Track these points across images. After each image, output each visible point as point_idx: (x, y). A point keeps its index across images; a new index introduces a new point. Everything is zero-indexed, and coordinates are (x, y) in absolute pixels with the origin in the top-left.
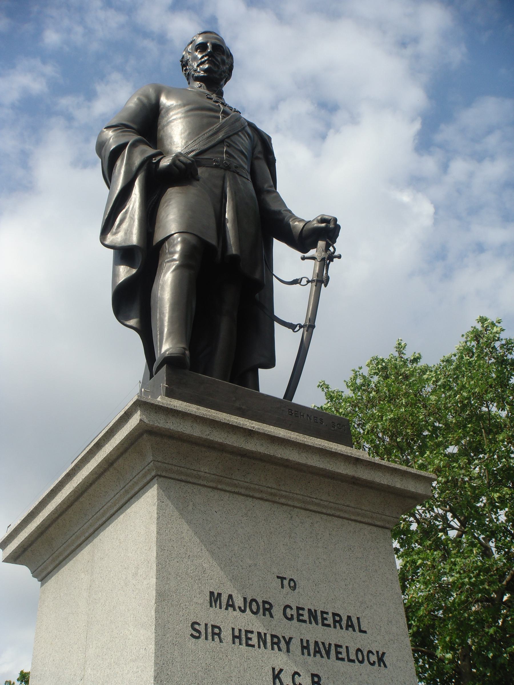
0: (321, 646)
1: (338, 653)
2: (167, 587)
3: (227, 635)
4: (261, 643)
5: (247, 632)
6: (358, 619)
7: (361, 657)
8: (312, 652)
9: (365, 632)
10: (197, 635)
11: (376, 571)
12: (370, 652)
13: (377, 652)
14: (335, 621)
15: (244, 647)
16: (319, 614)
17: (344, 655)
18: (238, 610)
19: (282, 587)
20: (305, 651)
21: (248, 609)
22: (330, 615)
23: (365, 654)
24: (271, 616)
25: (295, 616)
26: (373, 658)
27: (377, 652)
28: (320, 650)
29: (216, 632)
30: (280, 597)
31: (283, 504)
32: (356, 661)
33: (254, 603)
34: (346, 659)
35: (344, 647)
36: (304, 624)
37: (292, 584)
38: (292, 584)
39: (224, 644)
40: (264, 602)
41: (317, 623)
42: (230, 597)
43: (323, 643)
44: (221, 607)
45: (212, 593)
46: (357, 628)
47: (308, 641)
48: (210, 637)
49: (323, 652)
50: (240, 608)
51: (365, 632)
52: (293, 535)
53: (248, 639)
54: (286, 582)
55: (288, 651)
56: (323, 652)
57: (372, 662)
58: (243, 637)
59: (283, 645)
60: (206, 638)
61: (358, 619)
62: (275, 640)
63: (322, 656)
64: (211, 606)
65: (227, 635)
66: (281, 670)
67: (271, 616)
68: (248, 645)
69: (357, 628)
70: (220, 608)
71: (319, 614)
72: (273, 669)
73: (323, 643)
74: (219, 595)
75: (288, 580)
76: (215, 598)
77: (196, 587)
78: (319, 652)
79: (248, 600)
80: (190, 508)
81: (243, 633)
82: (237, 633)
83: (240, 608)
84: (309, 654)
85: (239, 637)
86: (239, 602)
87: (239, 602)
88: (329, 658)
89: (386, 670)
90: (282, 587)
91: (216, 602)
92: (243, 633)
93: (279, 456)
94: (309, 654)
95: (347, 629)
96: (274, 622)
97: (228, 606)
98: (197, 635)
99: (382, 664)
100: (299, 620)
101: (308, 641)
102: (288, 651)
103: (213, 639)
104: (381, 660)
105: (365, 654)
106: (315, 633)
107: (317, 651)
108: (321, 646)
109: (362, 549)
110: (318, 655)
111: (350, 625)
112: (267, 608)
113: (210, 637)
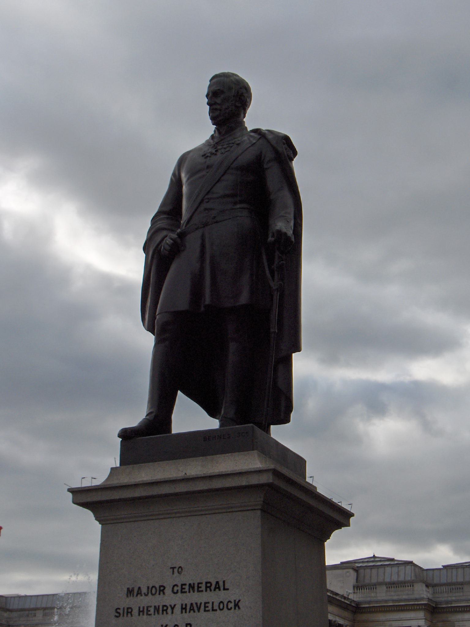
1: (205, 607)
3: (135, 611)
6: (224, 582)
7: (223, 606)
9: (228, 589)
12: (230, 602)
13: (235, 601)
14: (207, 587)
17: (210, 608)
19: (173, 573)
20: (184, 611)
21: (150, 594)
25: (179, 591)
26: (231, 605)
27: (235, 601)
28: (194, 608)
29: (129, 611)
30: (169, 581)
31: (179, 517)
32: (218, 610)
33: (154, 589)
36: (185, 594)
38: (180, 570)
42: (139, 588)
43: (196, 604)
44: (133, 596)
45: (128, 589)
46: (222, 588)
48: (125, 615)
49: (196, 609)
50: (144, 593)
51: (228, 589)
53: (148, 611)
54: (176, 570)
55: (172, 613)
56: (196, 609)
57: (229, 608)
58: (145, 610)
59: (169, 610)
60: (123, 615)
61: (224, 582)
63: (194, 612)
64: (127, 596)
65: (135, 611)
67: (164, 593)
68: (147, 614)
69: (222, 588)
73: (196, 604)
74: (133, 588)
76: (130, 592)
79: (150, 588)
83: (144, 593)
84: (186, 612)
85: (143, 611)
86: (144, 590)
87: (144, 590)
88: (199, 611)
90: (173, 573)
91: (130, 593)
99: (237, 608)
100: (182, 592)
102: (172, 613)
104: (237, 605)
107: (192, 609)
110: (192, 611)
111: (217, 587)
112: (162, 589)
113: (125, 615)
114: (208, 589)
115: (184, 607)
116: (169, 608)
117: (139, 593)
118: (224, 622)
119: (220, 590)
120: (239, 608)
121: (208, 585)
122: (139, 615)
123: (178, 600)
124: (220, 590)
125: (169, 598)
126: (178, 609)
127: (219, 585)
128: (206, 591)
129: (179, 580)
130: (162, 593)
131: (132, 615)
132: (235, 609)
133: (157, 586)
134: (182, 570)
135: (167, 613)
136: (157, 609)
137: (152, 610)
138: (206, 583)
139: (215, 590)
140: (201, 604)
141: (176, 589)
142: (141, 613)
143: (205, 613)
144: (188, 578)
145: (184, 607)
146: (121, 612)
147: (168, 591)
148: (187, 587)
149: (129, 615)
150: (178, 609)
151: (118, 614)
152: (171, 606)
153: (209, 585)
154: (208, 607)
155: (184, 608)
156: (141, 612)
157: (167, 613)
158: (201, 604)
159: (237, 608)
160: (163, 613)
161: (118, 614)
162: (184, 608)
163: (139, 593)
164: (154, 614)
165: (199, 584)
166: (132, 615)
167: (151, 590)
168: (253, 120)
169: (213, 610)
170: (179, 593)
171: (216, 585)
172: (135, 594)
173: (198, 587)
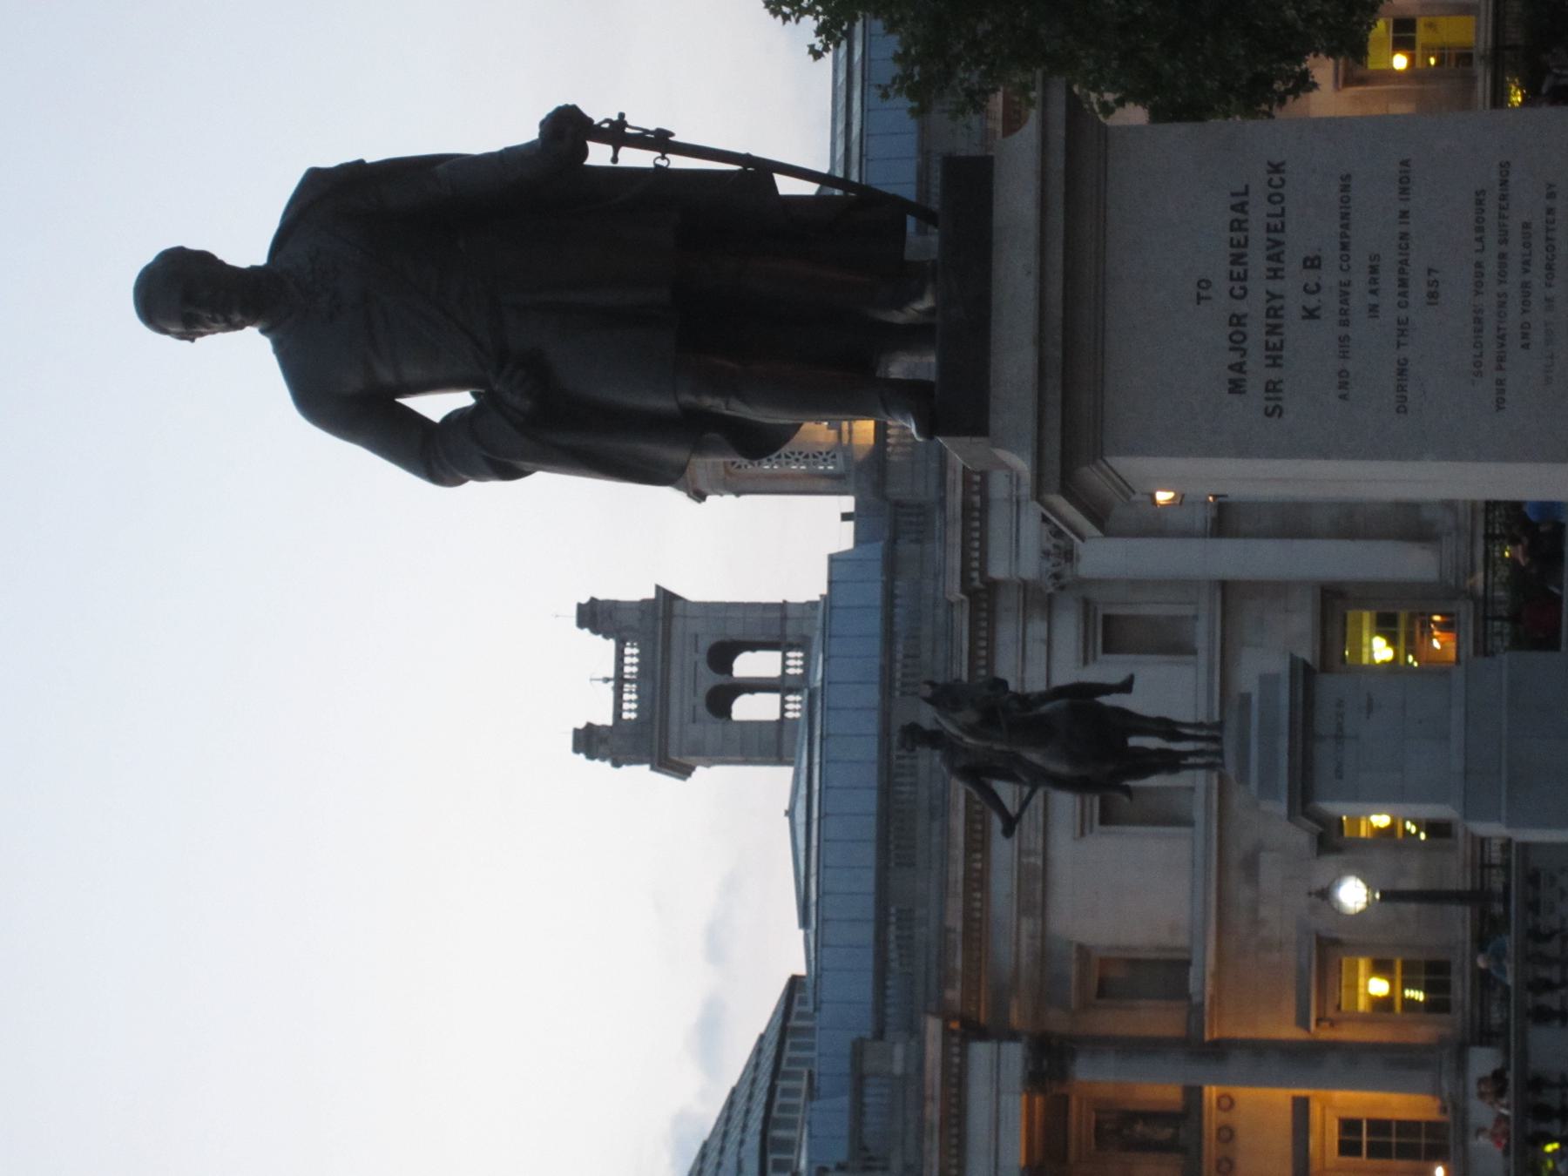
1: (1276, 230)
3: (1273, 374)
5: (1267, 348)
6: (1233, 195)
9: (1247, 187)
12: (1270, 183)
14: (1240, 229)
15: (1284, 353)
16: (1235, 251)
17: (1277, 221)
19: (1208, 298)
22: (1233, 234)
23: (1272, 190)
26: (1276, 179)
28: (1275, 253)
29: (1272, 387)
42: (1231, 367)
45: (1231, 391)
49: (1276, 250)
51: (1247, 187)
53: (1274, 348)
54: (1204, 293)
55: (1281, 297)
56: (1276, 250)
58: (1274, 353)
59: (1277, 303)
60: (1279, 399)
61: (1233, 195)
65: (1273, 374)
66: (1304, 308)
67: (1245, 316)
68: (1281, 348)
69: (1244, 198)
71: (1235, 251)
76: (1236, 387)
78: (1278, 255)
82: (1270, 362)
85: (1275, 358)
86: (1235, 357)
87: (1235, 357)
100: (1245, 278)
102: (1281, 297)
104: (1276, 168)
105: (1272, 190)
106: (1257, 260)
107: (1276, 258)
111: (1240, 207)
112: (1237, 320)
117: (1238, 367)
121: (1237, 226)
123: (1258, 286)
125: (1254, 306)
129: (1222, 285)
133: (1230, 330)
135: (1282, 308)
136: (1273, 330)
137: (1274, 339)
138: (1232, 230)
141: (1238, 292)
143: (1288, 228)
146: (1272, 404)
147: (1241, 307)
148: (1238, 269)
151: (1275, 412)
156: (1275, 362)
157: (1282, 308)
161: (1275, 412)
162: (1275, 274)
163: (1238, 367)
168: (246, 243)
169: (1283, 214)
170: (1248, 284)
173: (1239, 245)
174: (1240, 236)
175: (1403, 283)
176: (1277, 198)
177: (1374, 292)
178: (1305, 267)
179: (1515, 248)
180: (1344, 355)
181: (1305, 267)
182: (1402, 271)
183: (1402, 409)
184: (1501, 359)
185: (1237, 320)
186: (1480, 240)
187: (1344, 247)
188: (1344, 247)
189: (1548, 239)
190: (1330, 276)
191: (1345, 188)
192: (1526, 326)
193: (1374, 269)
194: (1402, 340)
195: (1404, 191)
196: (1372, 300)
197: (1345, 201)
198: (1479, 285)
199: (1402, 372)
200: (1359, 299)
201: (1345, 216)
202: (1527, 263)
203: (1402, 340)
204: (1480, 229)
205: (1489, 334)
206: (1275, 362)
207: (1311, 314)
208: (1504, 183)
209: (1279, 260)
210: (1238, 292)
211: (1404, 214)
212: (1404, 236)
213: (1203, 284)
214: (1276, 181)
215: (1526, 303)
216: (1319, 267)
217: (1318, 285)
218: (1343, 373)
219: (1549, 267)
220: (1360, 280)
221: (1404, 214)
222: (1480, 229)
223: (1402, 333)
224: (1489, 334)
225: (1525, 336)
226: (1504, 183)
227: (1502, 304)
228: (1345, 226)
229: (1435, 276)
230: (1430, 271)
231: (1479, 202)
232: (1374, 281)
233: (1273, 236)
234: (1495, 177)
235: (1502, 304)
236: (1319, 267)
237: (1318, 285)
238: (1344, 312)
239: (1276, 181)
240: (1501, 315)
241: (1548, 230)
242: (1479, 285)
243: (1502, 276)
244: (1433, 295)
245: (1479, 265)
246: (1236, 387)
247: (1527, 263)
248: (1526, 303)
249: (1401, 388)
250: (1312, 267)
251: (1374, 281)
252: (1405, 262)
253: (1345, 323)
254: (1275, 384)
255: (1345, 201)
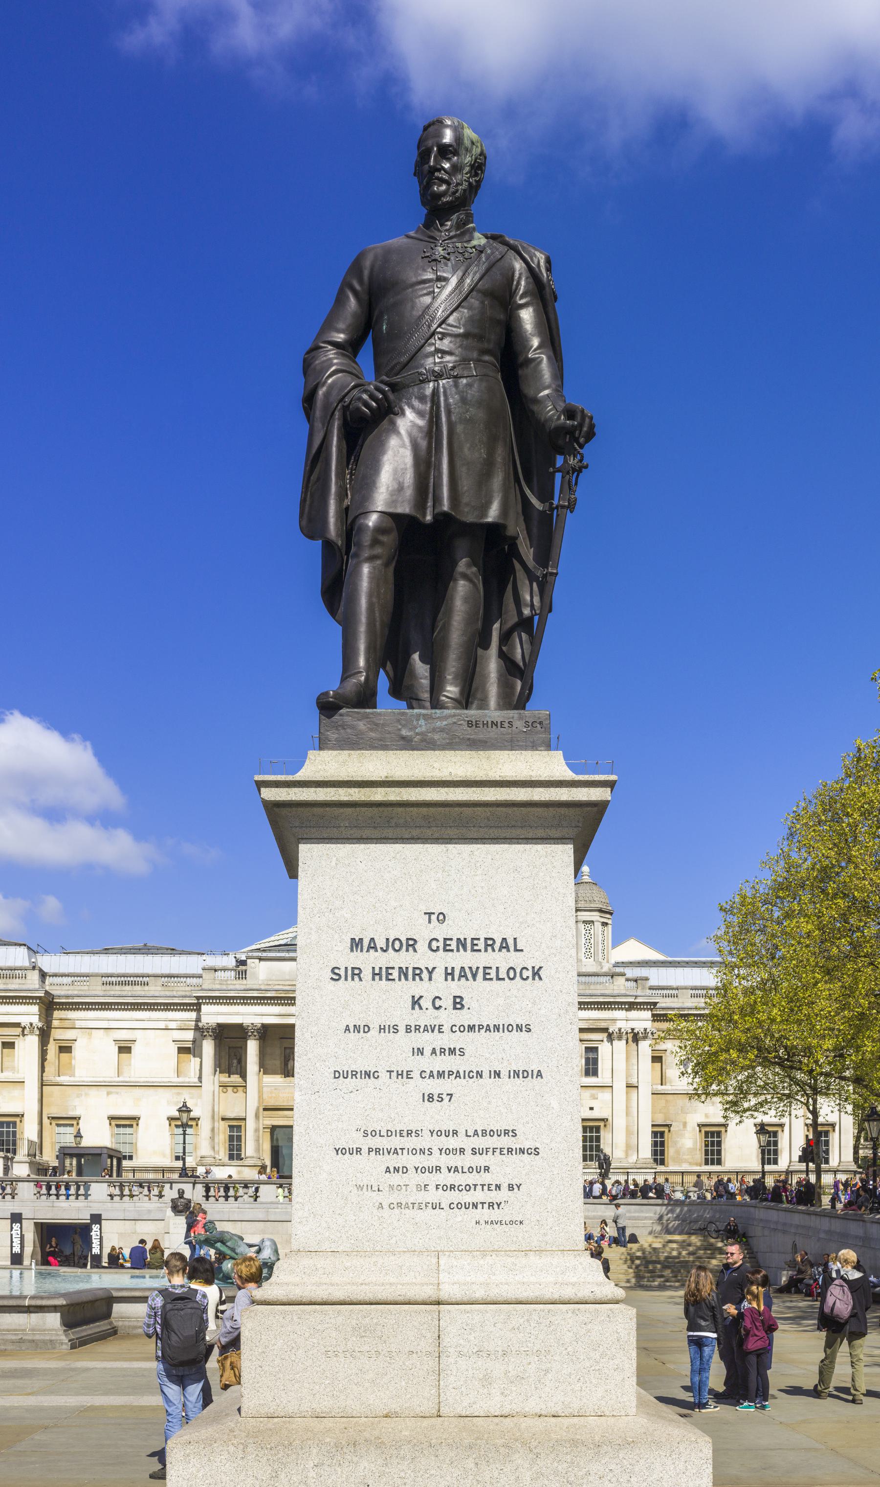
0: (467, 970)
1: (485, 974)
2: (309, 941)
3: (367, 974)
4: (403, 977)
6: (515, 939)
7: (512, 973)
8: (456, 977)
9: (522, 950)
10: (337, 977)
11: (546, 887)
13: (533, 968)
14: (487, 945)
17: (493, 975)
18: (379, 950)
19: (430, 922)
20: (449, 977)
22: (482, 940)
23: (518, 971)
24: (415, 951)
25: (441, 948)
26: (529, 973)
27: (533, 968)
29: (356, 973)
30: (424, 932)
32: (507, 979)
34: (495, 979)
35: (494, 969)
36: (450, 953)
37: (441, 917)
38: (441, 917)
39: (364, 982)
40: (408, 939)
41: (465, 950)
42: (372, 939)
43: (470, 968)
44: (362, 951)
45: (353, 940)
46: (512, 948)
47: (453, 968)
48: (349, 978)
51: (522, 950)
52: (447, 868)
54: (434, 917)
55: (430, 979)
58: (384, 973)
59: (425, 975)
60: (346, 979)
61: (515, 939)
62: (418, 972)
63: (467, 979)
64: (352, 950)
65: (367, 974)
67: (415, 951)
68: (388, 979)
69: (512, 948)
70: (362, 951)
72: (413, 997)
74: (361, 940)
75: (436, 915)
76: (356, 944)
77: (337, 936)
78: (465, 976)
79: (391, 941)
80: (333, 864)
81: (384, 970)
82: (377, 971)
84: (453, 979)
85: (380, 974)
86: (381, 943)
87: (381, 943)
88: (475, 980)
89: (541, 982)
90: (430, 922)
91: (357, 946)
92: (384, 970)
93: (414, 799)
94: (453, 979)
95: (500, 950)
96: (417, 955)
97: (369, 948)
98: (337, 977)
99: (537, 978)
100: (445, 950)
101: (453, 968)
102: (430, 979)
103: (353, 979)
104: (536, 974)
105: (518, 971)
107: (463, 975)
108: (467, 970)
109: (531, 867)
110: (463, 979)
112: (411, 944)
113: (349, 978)
114: (489, 948)
115: (449, 971)
116: (425, 971)
117: (372, 946)
118: (516, 997)
119: (508, 950)
120: (540, 978)
121: (489, 943)
122: (373, 979)
123: (441, 961)
124: (508, 950)
125: (422, 958)
126: (439, 975)
127: (507, 943)
128: (486, 950)
129: (440, 932)
130: (411, 949)
131: (361, 980)
132: (534, 979)
134: (444, 917)
135: (421, 979)
136: (403, 973)
137: (395, 974)
139: (500, 950)
140: (478, 968)
142: (377, 977)
144: (453, 930)
145: (449, 971)
147: (422, 946)
149: (356, 978)
150: (439, 975)
151: (335, 975)
152: (427, 968)
153: (490, 942)
154: (489, 974)
155: (449, 974)
156: (376, 974)
157: (421, 979)
158: (478, 968)
159: (537, 978)
160: (414, 979)
161: (335, 975)
163: (372, 946)
164: (400, 979)
165: (473, 939)
166: (361, 980)
167: (393, 945)
169: (498, 979)
171: (502, 943)
172: (365, 949)
173: (473, 945)
174: (481, 945)
175: (441, 1074)
176: (512, 975)
177: (434, 1051)
178: (455, 997)
179: (468, 1160)
180: (382, 1029)
181: (455, 997)
182: (450, 1073)
183: (337, 1075)
184: (377, 1151)
185: (411, 944)
186: (476, 1133)
187: (471, 1028)
188: (471, 1028)
189: (475, 1185)
190: (448, 1017)
191: (519, 1028)
192: (405, 1170)
193: (452, 1051)
194: (394, 1074)
195: (516, 1074)
196: (427, 1051)
197: (509, 1028)
198: (439, 1133)
199: (368, 1074)
200: (428, 1040)
201: (497, 1028)
202: (456, 1170)
203: (394, 1074)
204: (484, 1133)
205: (396, 1142)
206: (376, 974)
207: (416, 1002)
208: (522, 1151)
209: (460, 976)
210: (434, 945)
211: (498, 1074)
212: (480, 1074)
213: (442, 918)
214: (525, 974)
215: (424, 1170)
216: (455, 1008)
217: (440, 1007)
218: (367, 1029)
219: (452, 1187)
220: (446, 1040)
221: (498, 1074)
222: (484, 1133)
223: (400, 1074)
224: (396, 1142)
225: (396, 1170)
226: (522, 1151)
227: (422, 1152)
228: (488, 1029)
229: (446, 1098)
230: (451, 1095)
231: (506, 1132)
232: (443, 1051)
233: (481, 971)
234: (526, 1145)
235: (422, 1152)
236: (455, 1008)
237: (440, 1007)
238: (417, 1028)
239: (525, 974)
240: (414, 1152)
241: (483, 1185)
242: (439, 1133)
243: (448, 1152)
244: (431, 1098)
245: (455, 1133)
246: (356, 944)
247: (456, 1170)
248: (424, 1170)
249: (354, 1074)
250: (455, 1003)
251: (443, 1051)
252: (458, 1075)
253: (408, 1029)
254: (358, 975)
255: (509, 1028)
